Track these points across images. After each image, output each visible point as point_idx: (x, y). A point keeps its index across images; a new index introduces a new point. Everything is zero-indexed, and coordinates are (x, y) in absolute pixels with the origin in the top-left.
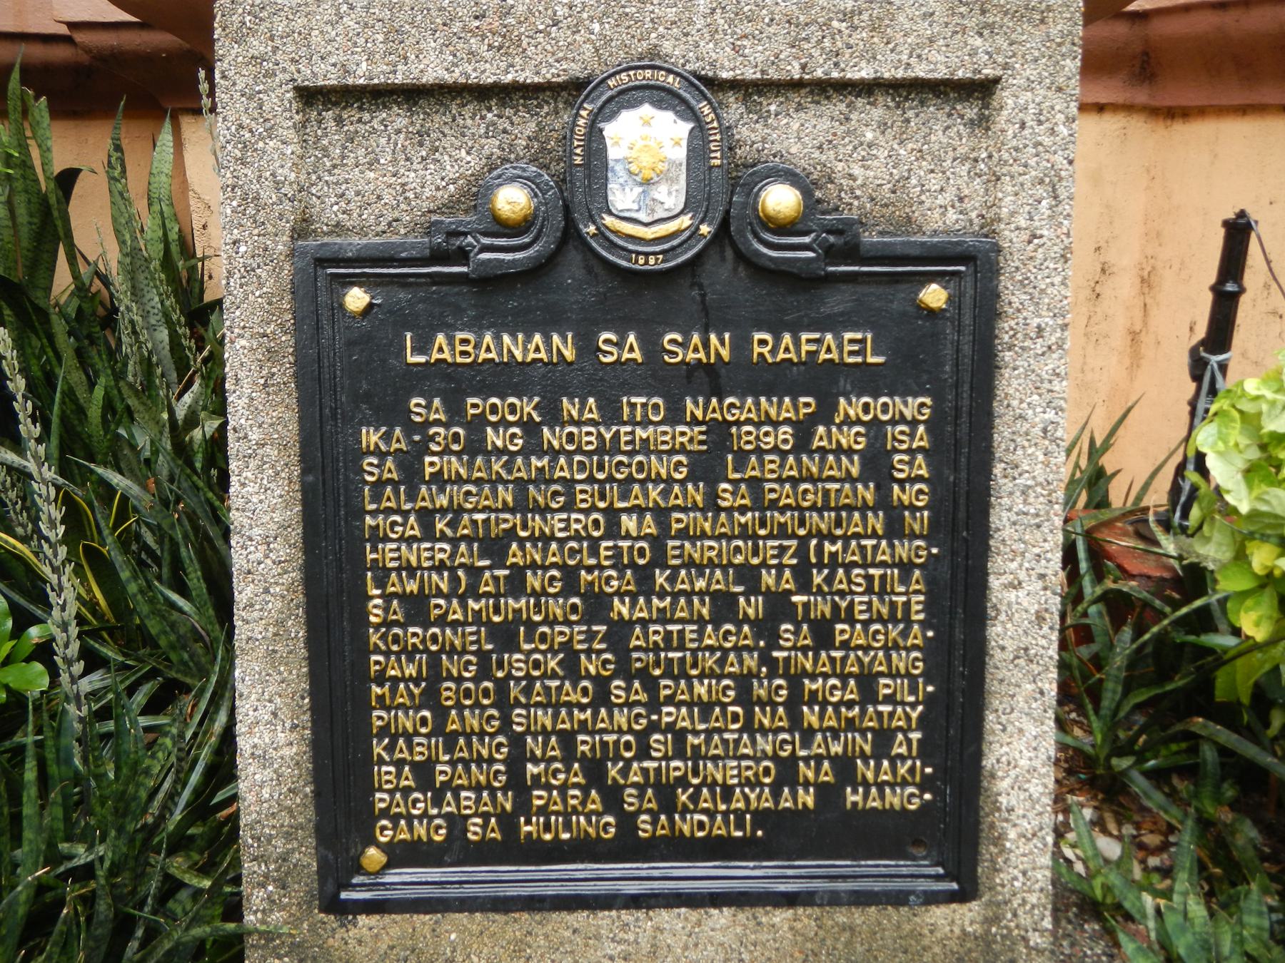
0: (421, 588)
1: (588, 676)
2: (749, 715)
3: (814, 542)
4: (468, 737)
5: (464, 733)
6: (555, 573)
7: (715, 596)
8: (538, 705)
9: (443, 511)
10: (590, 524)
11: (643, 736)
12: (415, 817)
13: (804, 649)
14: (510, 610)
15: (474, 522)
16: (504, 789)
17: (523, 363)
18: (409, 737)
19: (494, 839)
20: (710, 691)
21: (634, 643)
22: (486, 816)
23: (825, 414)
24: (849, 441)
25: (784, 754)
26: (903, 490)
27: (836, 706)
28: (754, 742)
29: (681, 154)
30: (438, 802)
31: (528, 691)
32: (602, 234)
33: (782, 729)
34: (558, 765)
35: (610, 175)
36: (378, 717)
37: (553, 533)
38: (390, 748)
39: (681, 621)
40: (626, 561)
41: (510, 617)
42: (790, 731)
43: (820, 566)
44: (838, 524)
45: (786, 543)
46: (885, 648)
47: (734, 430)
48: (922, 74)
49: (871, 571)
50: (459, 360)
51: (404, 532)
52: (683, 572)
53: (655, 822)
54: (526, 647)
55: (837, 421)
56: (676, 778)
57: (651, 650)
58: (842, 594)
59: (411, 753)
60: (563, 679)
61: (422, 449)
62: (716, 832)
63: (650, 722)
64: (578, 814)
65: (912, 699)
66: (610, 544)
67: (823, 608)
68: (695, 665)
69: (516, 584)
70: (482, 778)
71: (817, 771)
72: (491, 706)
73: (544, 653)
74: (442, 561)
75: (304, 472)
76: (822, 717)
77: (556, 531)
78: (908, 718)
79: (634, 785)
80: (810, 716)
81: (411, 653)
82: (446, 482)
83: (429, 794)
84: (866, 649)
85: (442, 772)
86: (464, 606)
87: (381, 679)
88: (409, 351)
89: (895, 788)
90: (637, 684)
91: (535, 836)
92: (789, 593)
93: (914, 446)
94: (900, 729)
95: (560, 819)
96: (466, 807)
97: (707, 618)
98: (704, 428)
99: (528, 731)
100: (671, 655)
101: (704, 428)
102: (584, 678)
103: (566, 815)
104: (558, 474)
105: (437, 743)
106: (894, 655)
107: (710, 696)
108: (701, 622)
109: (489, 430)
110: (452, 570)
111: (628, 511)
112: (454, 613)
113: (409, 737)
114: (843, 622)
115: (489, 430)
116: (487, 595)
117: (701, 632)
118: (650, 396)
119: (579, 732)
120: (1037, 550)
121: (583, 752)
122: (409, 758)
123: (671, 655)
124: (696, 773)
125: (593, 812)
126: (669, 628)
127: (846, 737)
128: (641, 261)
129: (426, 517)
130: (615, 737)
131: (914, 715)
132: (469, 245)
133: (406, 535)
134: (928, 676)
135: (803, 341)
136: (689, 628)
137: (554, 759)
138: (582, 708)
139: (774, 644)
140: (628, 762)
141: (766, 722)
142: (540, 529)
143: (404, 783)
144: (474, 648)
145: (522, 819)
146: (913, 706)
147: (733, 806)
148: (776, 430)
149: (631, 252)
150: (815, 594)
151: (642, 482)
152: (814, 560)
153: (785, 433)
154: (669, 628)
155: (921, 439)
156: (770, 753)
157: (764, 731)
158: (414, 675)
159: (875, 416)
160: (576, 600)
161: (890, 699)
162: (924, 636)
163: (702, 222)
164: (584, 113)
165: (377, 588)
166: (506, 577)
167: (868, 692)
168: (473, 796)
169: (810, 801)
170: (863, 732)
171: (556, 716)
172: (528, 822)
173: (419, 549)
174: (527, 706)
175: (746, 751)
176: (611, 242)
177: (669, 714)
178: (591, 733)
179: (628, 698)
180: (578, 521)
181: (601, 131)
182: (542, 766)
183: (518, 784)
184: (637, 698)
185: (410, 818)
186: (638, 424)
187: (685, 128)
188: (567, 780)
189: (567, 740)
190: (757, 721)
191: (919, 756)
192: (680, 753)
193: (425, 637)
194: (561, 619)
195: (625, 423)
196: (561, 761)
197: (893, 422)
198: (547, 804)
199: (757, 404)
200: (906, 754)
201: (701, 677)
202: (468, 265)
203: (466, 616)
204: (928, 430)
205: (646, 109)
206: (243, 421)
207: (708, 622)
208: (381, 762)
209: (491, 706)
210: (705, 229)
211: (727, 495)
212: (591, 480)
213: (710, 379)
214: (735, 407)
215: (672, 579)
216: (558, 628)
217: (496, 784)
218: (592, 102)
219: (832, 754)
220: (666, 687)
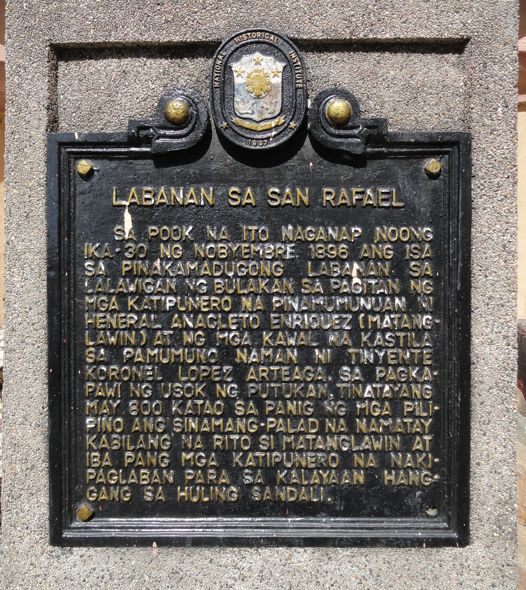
0: (118, 341)
1: (221, 398)
2: (322, 425)
3: (362, 315)
4: (146, 434)
5: (143, 432)
6: (200, 333)
7: (300, 348)
8: (189, 415)
9: (132, 294)
10: (223, 303)
11: (255, 436)
12: (112, 485)
13: (357, 382)
14: (173, 356)
15: (152, 301)
16: (168, 468)
17: (182, 206)
18: (108, 434)
19: (161, 500)
20: (297, 409)
21: (250, 377)
22: (155, 485)
23: (368, 237)
24: (382, 254)
25: (345, 449)
26: (417, 283)
27: (377, 418)
28: (325, 441)
29: (278, 80)
30: (126, 476)
31: (182, 406)
32: (231, 128)
33: (342, 433)
34: (203, 454)
35: (235, 93)
36: (90, 422)
37: (199, 308)
38: (97, 441)
39: (279, 364)
40: (245, 327)
41: (173, 360)
42: (347, 434)
43: (366, 330)
44: (377, 303)
45: (344, 316)
46: (408, 382)
47: (312, 246)
48: (423, 36)
49: (398, 334)
50: (144, 203)
51: (108, 307)
52: (280, 334)
53: (262, 492)
54: (184, 379)
55: (375, 242)
56: (277, 463)
57: (261, 382)
58: (380, 348)
59: (110, 446)
60: (205, 399)
61: (120, 256)
62: (301, 498)
63: (260, 427)
64: (214, 485)
65: (425, 414)
66: (235, 315)
67: (367, 356)
68: (288, 392)
69: (177, 339)
70: (154, 461)
71: (366, 460)
72: (160, 415)
73: (193, 382)
74: (131, 325)
75: (49, 269)
76: (368, 426)
77: (202, 307)
78: (423, 425)
79: (249, 467)
80: (362, 424)
81: (110, 381)
82: (136, 276)
83: (121, 471)
84: (394, 382)
85: (129, 457)
86: (144, 353)
87: (92, 397)
88: (114, 198)
89: (416, 473)
90: (251, 404)
91: (186, 499)
92: (347, 347)
93: (423, 256)
94: (417, 433)
95: (203, 488)
96: (143, 480)
97: (295, 362)
98: (293, 245)
99: (182, 432)
100: (272, 385)
101: (293, 245)
102: (218, 399)
103: (207, 486)
104: (203, 272)
105: (126, 438)
106: (413, 386)
107: (297, 412)
108: (291, 363)
109: (162, 245)
110: (138, 330)
111: (247, 295)
112: (138, 357)
113: (108, 434)
114: (380, 365)
115: (162, 245)
116: (158, 346)
117: (291, 371)
118: (260, 225)
119: (215, 433)
120: (502, 321)
121: (217, 446)
122: (109, 448)
123: (272, 385)
124: (289, 459)
125: (223, 484)
126: (272, 368)
127: (384, 439)
128: (254, 144)
129: (122, 297)
130: (237, 437)
131: (427, 424)
132: (152, 134)
133: (110, 309)
134: (435, 400)
135: (354, 193)
136: (284, 368)
137: (198, 450)
138: (217, 417)
139: (337, 378)
140: (246, 452)
141: (333, 429)
142: (192, 306)
143: (105, 463)
144: (150, 379)
145: (179, 488)
146: (426, 418)
147: (312, 482)
148: (337, 247)
149: (248, 138)
150: (362, 348)
151: (256, 277)
152: (362, 327)
153: (343, 248)
154: (272, 368)
155: (428, 252)
156: (335, 448)
157: (331, 434)
158: (113, 395)
159: (399, 238)
160: (214, 351)
161: (411, 414)
162: (432, 375)
163: (291, 120)
164: (220, 57)
165: (92, 341)
166: (171, 335)
167: (397, 411)
168: (148, 473)
169: (362, 480)
170: (394, 435)
171: (200, 423)
172: (182, 490)
173: (117, 317)
174: (182, 416)
175: (321, 447)
176: (236, 132)
177: (272, 422)
178: (223, 434)
179: (245, 412)
180: (215, 301)
181: (231, 68)
182: (192, 454)
183: (176, 464)
184: (251, 412)
185: (108, 485)
186: (253, 242)
187: (280, 66)
188: (206, 464)
189: (207, 436)
190: (327, 428)
191: (432, 450)
192: (278, 448)
193: (120, 371)
194: (204, 362)
195: (245, 242)
196: (204, 451)
197: (410, 242)
198: (194, 479)
199: (327, 231)
200: (422, 449)
201: (291, 399)
202: (151, 147)
203: (145, 360)
204: (431, 247)
205: (257, 55)
206: (13, 238)
207: (296, 365)
208: (91, 450)
209: (160, 415)
210: (292, 125)
211: (307, 286)
212: (223, 276)
213: (298, 215)
214: (310, 232)
215: (274, 338)
216: (203, 367)
217: (163, 465)
218: (225, 51)
219: (375, 449)
220: (270, 405)
